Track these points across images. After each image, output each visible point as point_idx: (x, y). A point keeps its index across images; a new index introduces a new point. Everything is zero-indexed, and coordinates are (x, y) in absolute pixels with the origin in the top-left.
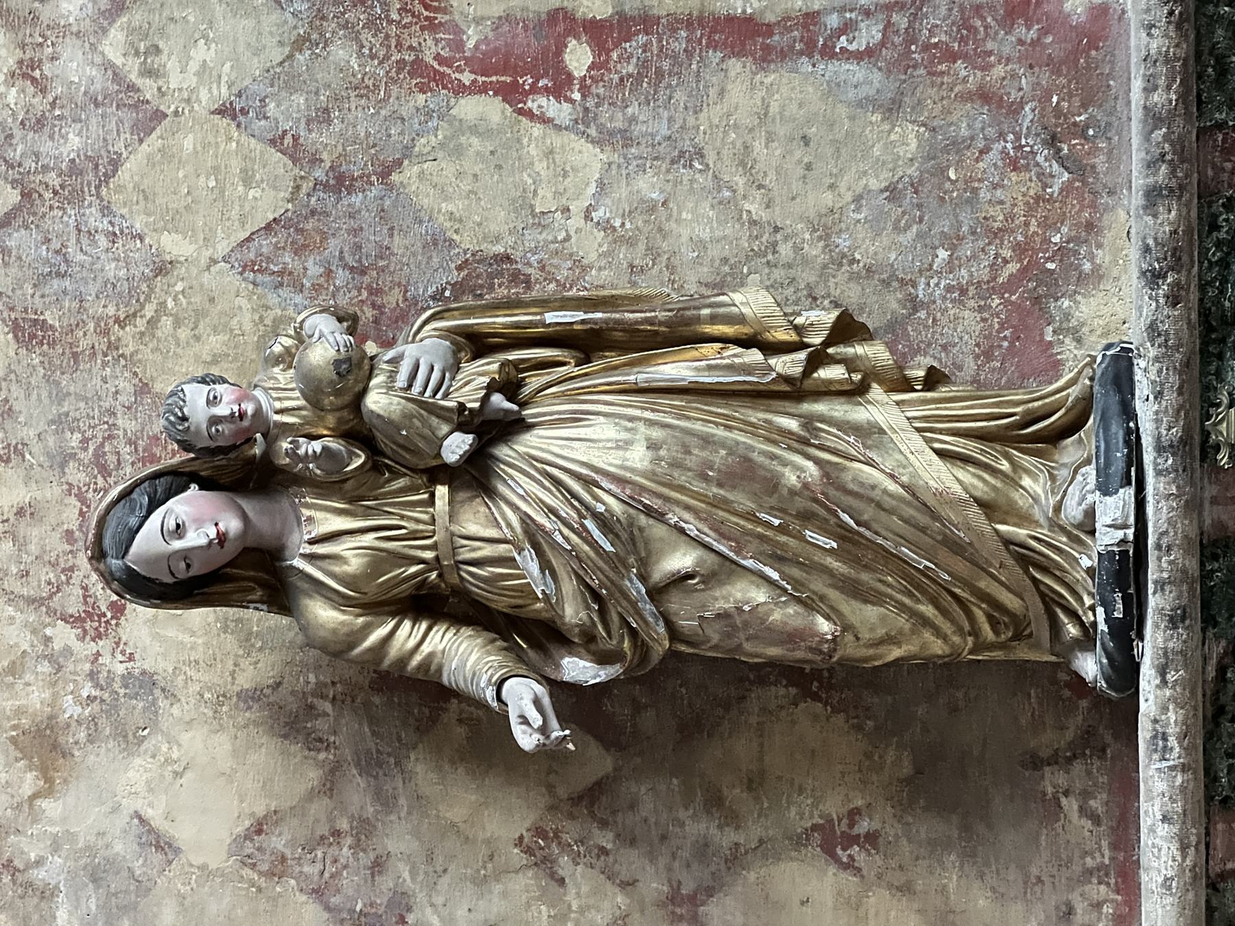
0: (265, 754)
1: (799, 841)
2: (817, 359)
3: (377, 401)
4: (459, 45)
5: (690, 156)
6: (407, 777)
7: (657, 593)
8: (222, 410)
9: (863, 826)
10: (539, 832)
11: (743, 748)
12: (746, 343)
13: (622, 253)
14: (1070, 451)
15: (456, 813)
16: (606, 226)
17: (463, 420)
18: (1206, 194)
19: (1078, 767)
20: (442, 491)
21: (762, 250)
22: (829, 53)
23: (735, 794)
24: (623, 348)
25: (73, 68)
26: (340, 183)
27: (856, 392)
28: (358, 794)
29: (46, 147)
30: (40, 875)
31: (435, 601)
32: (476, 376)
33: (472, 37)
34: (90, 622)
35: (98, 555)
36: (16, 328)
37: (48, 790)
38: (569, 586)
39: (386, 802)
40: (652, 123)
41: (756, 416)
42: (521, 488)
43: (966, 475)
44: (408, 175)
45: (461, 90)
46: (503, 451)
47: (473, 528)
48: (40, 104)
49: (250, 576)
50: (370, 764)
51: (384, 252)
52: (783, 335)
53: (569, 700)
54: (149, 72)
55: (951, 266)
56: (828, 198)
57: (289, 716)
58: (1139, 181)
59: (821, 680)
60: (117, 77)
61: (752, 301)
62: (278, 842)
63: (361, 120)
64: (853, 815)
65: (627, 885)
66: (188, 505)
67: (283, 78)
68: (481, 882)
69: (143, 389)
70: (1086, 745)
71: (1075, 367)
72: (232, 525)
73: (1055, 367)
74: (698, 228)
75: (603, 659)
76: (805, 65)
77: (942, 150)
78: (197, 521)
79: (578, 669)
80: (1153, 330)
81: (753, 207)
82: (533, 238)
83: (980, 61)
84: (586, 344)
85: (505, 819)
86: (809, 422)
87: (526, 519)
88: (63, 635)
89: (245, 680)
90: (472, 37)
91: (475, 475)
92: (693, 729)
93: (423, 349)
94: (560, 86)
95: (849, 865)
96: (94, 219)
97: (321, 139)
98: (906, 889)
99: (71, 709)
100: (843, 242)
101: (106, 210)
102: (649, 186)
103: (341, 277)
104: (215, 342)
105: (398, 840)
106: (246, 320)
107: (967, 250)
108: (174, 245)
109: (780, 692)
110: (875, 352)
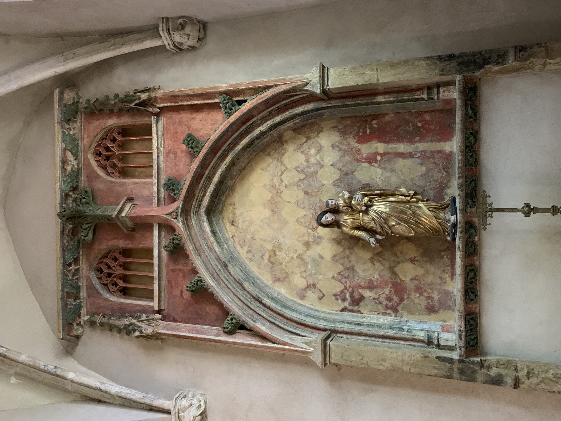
0: (335, 246)
1: (407, 260)
2: (412, 198)
3: (353, 202)
4: (362, 157)
5: (394, 171)
6: (354, 250)
7: (390, 227)
8: (333, 203)
9: (416, 259)
10: (372, 258)
11: (400, 248)
12: (402, 195)
13: (384, 183)
14: (447, 210)
15: (360, 255)
16: (382, 180)
17: (365, 205)
18: (466, 177)
19: (446, 252)
20: (361, 214)
21: (404, 184)
22: (413, 157)
23: (399, 254)
24: (385, 196)
25: (313, 160)
26: (346, 174)
27: (417, 202)
28: (347, 252)
29: (309, 170)
30: (307, 261)
31: (358, 228)
32: (366, 200)
33: (364, 156)
34: (314, 229)
35: (317, 221)
36: (305, 192)
37: (308, 250)
38: (378, 226)
39: (351, 253)
40: (388, 166)
41: (403, 205)
42: (372, 214)
43: (433, 213)
44: (355, 173)
45: (363, 162)
46: (369, 209)
47: (365, 218)
48: (308, 164)
49: (336, 224)
50: (349, 248)
51: (352, 183)
52: (407, 194)
53: (377, 241)
54: (322, 160)
55: (430, 185)
56: (413, 176)
57: (338, 242)
58: (457, 176)
59: (408, 239)
60: (318, 161)
61: (403, 190)
62: (337, 258)
63: (350, 166)
64: (415, 257)
65: (383, 265)
66: (328, 215)
67: (339, 161)
68: (364, 264)
69: (320, 200)
70: (448, 249)
71: (447, 199)
72: (334, 217)
73: (444, 199)
74: (394, 180)
75: (382, 236)
76: (410, 159)
77: (428, 170)
78: (329, 217)
79: (378, 237)
80: (459, 195)
81: (402, 177)
82: (372, 181)
83: (434, 158)
84: (380, 196)
85: (368, 255)
86: (410, 206)
87: (373, 218)
88: (310, 231)
89: (333, 237)
90: (364, 156)
91: (366, 212)
92: (393, 245)
93: (359, 195)
94: (376, 161)
95: (414, 264)
96: (315, 179)
97: (344, 169)
98: (421, 267)
99: (311, 240)
100: (415, 182)
101: (316, 178)
102: (388, 175)
103: (346, 186)
104: (329, 194)
105: (353, 258)
106: (334, 191)
107: (432, 183)
108: (325, 182)
109: (405, 241)
110: (419, 197)
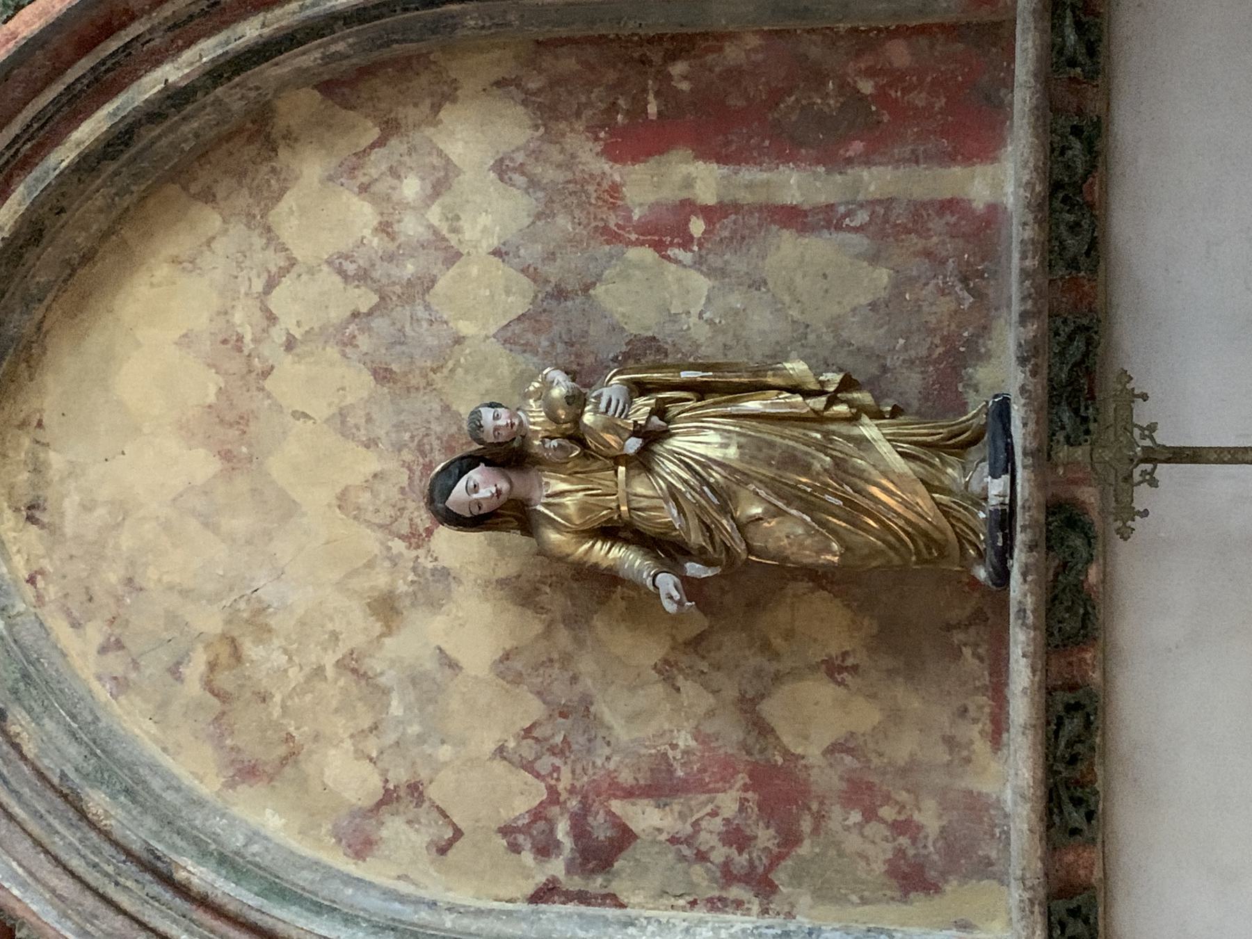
0: (512, 614)
1: (813, 668)
3: (588, 418)
4: (629, 218)
5: (758, 284)
7: (741, 527)
8: (502, 422)
9: (850, 661)
10: (666, 661)
11: (782, 615)
12: (793, 390)
14: (974, 454)
16: (710, 322)
17: (638, 431)
18: (1052, 315)
19: (972, 630)
20: (622, 469)
21: (800, 339)
22: (839, 227)
23: (777, 642)
25: (410, 227)
27: (853, 419)
28: (563, 636)
29: (394, 271)
30: (382, 680)
31: (610, 532)
32: (642, 408)
33: (636, 216)
34: (417, 539)
35: (431, 501)
36: (375, 373)
37: (388, 632)
38: (694, 523)
39: (579, 642)
40: (738, 263)
41: (797, 432)
42: (669, 469)
43: (915, 466)
44: (599, 291)
46: (657, 448)
47: (640, 490)
48: (392, 247)
49: (512, 516)
52: (813, 386)
53: (691, 587)
54: (454, 230)
55: (905, 348)
56: (836, 310)
57: (522, 593)
58: (1016, 308)
60: (436, 232)
61: (797, 368)
62: (518, 665)
64: (845, 655)
65: (715, 692)
66: (476, 475)
67: (529, 234)
68: (632, 689)
70: (978, 617)
71: (976, 408)
74: (762, 324)
75: (708, 563)
77: (900, 284)
78: (482, 486)
79: (694, 569)
80: (1023, 390)
81: (795, 313)
82: (669, 328)
83: (924, 233)
84: (701, 390)
86: (826, 434)
88: (398, 546)
89: (501, 573)
90: (636, 216)
91: (643, 462)
92: (754, 605)
93: (612, 388)
95: (842, 683)
96: (420, 312)
98: (873, 696)
99: (402, 587)
100: (845, 334)
101: (427, 307)
102: (736, 300)
103: (560, 347)
104: (487, 383)
105: (586, 665)
106: (505, 370)
107: (915, 339)
108: (465, 327)
109: (803, 586)
110: (864, 397)
